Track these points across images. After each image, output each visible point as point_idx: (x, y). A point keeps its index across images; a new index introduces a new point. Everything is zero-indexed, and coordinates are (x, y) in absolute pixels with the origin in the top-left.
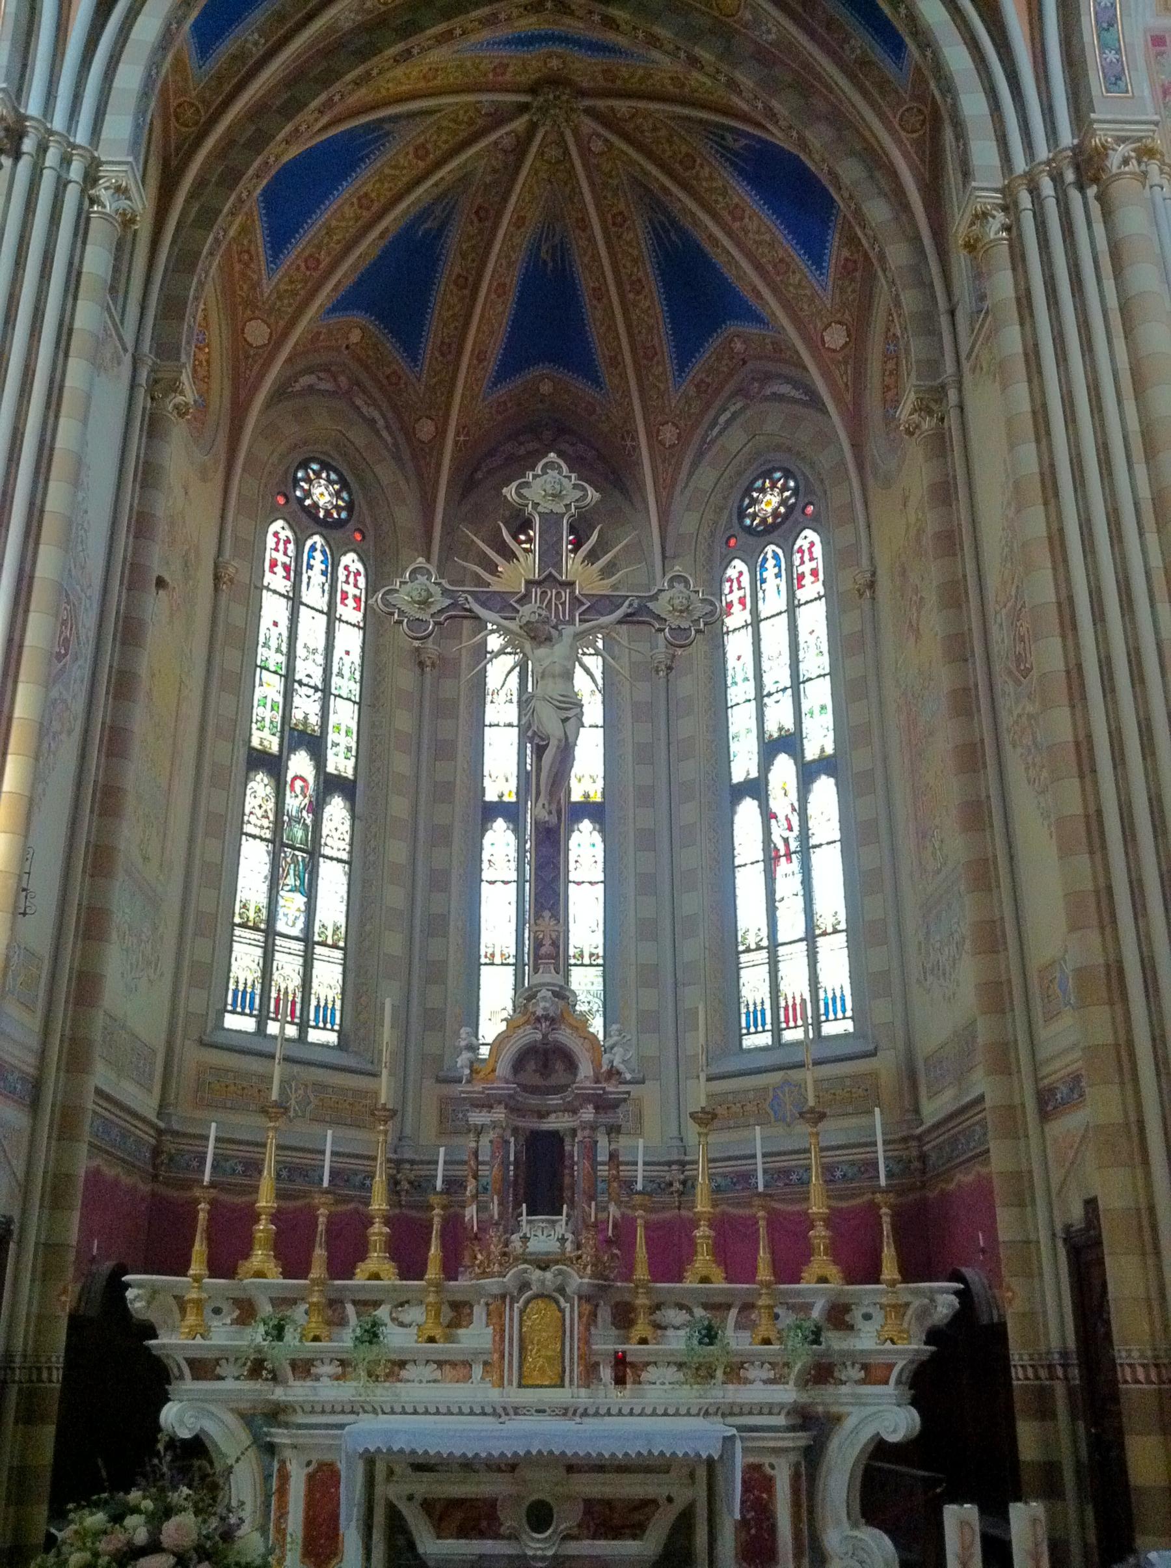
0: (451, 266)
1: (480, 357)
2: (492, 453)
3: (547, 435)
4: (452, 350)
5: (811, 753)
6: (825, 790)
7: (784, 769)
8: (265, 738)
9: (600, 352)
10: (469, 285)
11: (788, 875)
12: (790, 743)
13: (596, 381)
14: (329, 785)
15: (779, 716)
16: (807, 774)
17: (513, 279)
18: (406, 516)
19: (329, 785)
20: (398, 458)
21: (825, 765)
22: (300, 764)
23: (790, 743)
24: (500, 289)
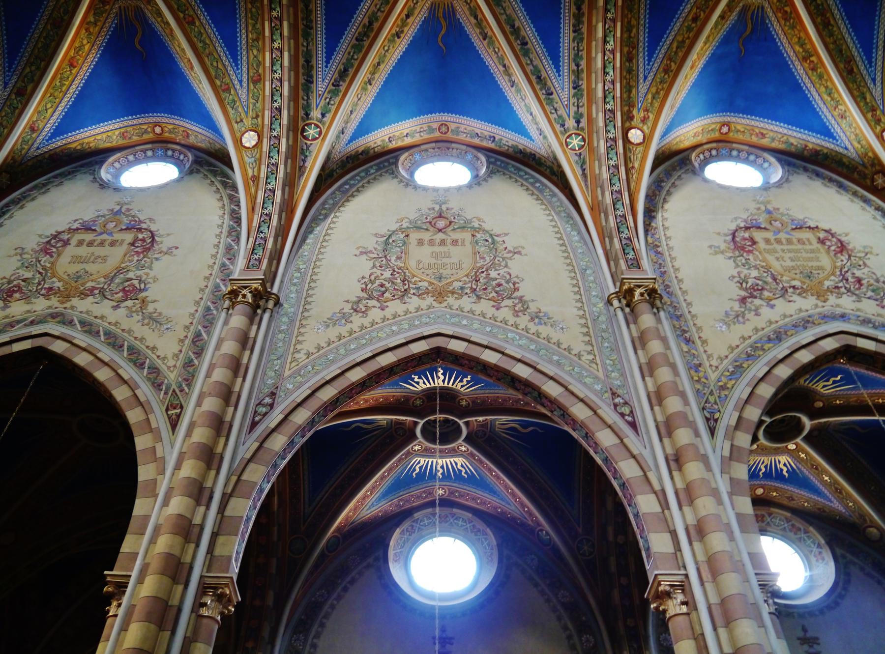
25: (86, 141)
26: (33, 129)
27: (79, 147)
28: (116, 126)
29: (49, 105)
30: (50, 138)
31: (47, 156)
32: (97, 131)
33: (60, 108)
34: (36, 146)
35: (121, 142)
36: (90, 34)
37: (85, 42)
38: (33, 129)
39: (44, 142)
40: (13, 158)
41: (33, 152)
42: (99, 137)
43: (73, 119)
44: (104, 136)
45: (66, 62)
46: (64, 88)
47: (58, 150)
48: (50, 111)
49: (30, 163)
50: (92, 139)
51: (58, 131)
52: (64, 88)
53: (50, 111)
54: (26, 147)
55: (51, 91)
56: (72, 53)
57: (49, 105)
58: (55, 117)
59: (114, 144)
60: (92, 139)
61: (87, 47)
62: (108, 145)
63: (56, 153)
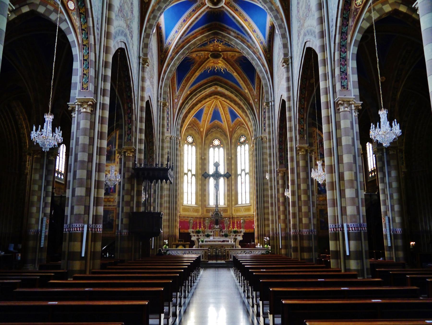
0: (205, 112)
1: (208, 121)
2: (209, 131)
4: (205, 121)
5: (246, 172)
6: (247, 176)
7: (243, 173)
8: (186, 171)
9: (223, 120)
10: (207, 114)
11: (243, 185)
12: (244, 170)
13: (222, 122)
14: (192, 175)
15: (243, 168)
16: (246, 174)
17: (212, 113)
18: (200, 141)
19: (192, 175)
21: (248, 173)
22: (189, 174)
23: (244, 170)
24: (210, 114)
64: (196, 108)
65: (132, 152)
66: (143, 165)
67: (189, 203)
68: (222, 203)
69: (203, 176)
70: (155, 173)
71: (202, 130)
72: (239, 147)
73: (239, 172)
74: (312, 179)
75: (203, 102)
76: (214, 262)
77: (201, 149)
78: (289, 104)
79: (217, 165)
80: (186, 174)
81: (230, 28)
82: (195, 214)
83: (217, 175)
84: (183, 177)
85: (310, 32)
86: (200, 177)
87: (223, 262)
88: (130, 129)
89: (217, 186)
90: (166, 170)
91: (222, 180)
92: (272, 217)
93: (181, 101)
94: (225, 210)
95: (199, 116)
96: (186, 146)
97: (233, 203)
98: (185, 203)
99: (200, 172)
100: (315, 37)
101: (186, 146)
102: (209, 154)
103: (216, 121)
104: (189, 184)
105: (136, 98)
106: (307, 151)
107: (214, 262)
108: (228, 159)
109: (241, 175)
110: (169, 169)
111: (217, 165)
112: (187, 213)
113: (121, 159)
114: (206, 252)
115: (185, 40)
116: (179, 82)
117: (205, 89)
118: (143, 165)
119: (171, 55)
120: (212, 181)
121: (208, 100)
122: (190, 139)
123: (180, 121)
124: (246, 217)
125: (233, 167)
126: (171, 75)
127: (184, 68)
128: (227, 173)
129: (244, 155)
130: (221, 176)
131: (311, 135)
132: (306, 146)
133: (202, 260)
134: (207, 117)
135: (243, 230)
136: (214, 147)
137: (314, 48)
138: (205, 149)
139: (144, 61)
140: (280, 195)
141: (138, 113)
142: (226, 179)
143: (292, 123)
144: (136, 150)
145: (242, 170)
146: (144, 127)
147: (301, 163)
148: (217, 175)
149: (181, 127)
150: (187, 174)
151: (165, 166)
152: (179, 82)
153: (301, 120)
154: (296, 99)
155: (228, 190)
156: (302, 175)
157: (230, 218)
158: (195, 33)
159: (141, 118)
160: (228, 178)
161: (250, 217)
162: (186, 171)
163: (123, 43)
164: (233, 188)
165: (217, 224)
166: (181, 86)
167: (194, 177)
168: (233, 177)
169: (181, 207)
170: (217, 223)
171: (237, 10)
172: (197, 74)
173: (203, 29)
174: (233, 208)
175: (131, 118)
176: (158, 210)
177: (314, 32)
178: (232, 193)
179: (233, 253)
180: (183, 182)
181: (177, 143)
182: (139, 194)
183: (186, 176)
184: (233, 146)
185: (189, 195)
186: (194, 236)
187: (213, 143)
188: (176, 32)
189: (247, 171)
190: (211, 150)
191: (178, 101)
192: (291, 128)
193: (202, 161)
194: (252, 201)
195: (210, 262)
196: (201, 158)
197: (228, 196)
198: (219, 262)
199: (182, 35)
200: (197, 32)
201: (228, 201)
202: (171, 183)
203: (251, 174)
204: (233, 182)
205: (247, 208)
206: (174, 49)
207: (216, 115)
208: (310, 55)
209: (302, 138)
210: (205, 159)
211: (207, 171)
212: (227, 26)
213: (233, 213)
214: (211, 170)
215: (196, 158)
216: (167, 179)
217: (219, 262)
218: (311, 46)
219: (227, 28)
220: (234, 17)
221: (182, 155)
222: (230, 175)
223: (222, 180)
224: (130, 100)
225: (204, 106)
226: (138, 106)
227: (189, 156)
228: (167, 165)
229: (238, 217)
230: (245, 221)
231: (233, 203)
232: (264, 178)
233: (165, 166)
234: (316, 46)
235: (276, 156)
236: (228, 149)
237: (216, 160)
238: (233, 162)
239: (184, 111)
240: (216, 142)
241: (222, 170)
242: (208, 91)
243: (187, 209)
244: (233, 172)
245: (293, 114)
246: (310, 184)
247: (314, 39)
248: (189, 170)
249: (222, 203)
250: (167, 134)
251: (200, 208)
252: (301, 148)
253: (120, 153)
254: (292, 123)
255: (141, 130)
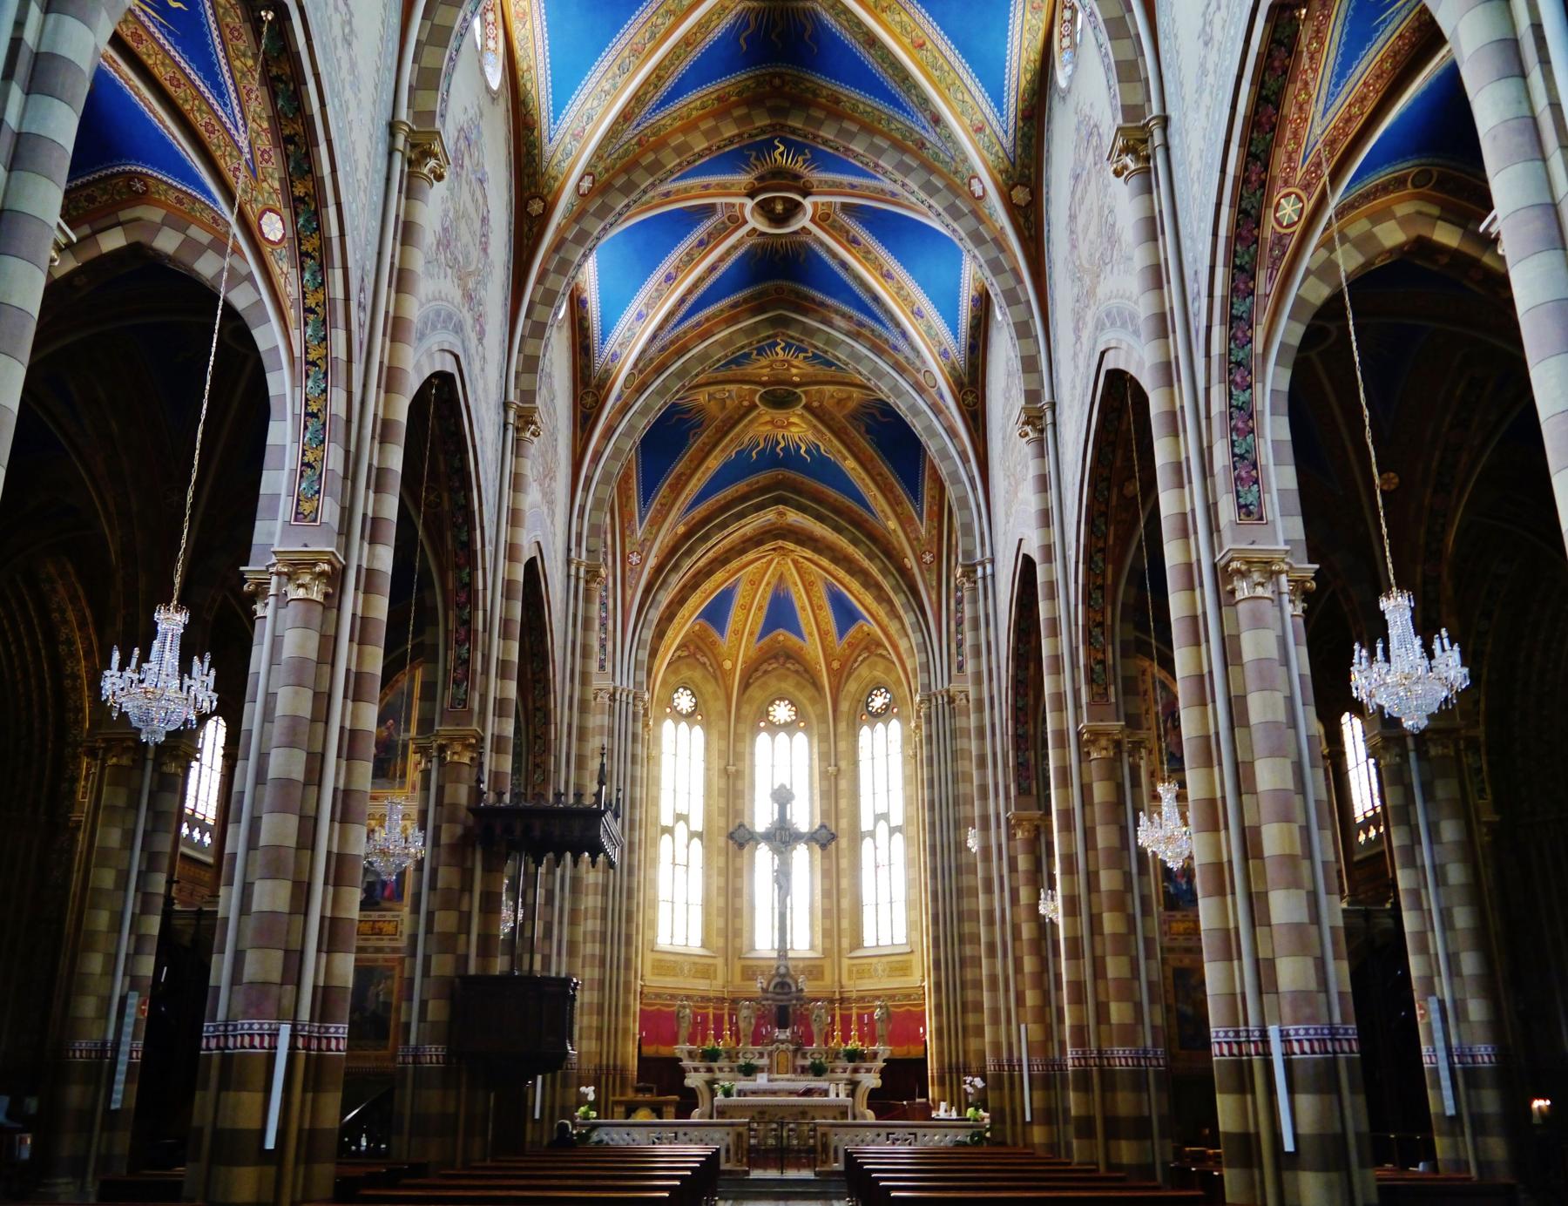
0: (738, 600)
1: (751, 634)
2: (756, 670)
3: (781, 660)
4: (738, 633)
6: (898, 837)
7: (882, 828)
9: (805, 632)
11: (883, 872)
12: (885, 817)
13: (802, 637)
14: (692, 835)
15: (881, 809)
16: (892, 831)
18: (720, 705)
19: (692, 835)
20: (716, 679)
21: (898, 829)
22: (681, 829)
23: (885, 817)
24: (760, 608)
25: (1023, 63)
26: (980, 130)
27: (1029, 76)
28: (1019, 14)
29: (959, 96)
30: (1000, 110)
31: (1021, 124)
32: (1016, 43)
33: (969, 82)
34: (1001, 134)
35: (1044, 15)
36: (889, 7)
37: (897, 18)
38: (980, 130)
39: (1003, 125)
40: (1001, 172)
41: (1008, 142)
42: (1026, 44)
43: (990, 75)
44: (1027, 35)
45: (915, 52)
46: (946, 68)
47: (1020, 106)
48: (967, 97)
49: (1019, 151)
50: (1024, 55)
51: (997, 98)
52: (946, 68)
53: (967, 97)
54: (998, 147)
55: (942, 86)
56: (907, 41)
57: (959, 96)
58: (977, 94)
59: (1043, 26)
60: (1024, 55)
61: (905, 18)
62: (1041, 36)
63: (1023, 111)
64: (707, 585)
65: (468, 746)
66: (507, 798)
67: (679, 940)
68: (802, 942)
69: (732, 839)
70: (547, 827)
71: (728, 665)
72: (865, 731)
73: (866, 824)
74: (1142, 853)
75: (735, 564)
76: (772, 1174)
77: (725, 735)
78: (1049, 572)
79: (782, 797)
80: (669, 831)
81: (830, 301)
82: (701, 986)
83: (783, 837)
84: (655, 844)
85: (1115, 318)
86: (721, 841)
87: (807, 1174)
88: (465, 663)
89: (783, 878)
90: (595, 816)
91: (801, 855)
92: (994, 999)
93: (652, 562)
94: (814, 970)
95: (716, 614)
96: (668, 725)
97: (845, 943)
98: (663, 941)
99: (722, 822)
100: (1136, 333)
101: (668, 725)
102: (752, 754)
103: (782, 635)
104: (680, 870)
105: (489, 549)
106: (1118, 744)
107: (772, 1174)
108: (824, 775)
109: (872, 834)
110: (604, 812)
111: (782, 797)
112: (669, 982)
113: (426, 774)
114: (739, 1135)
115: (672, 343)
116: (647, 493)
117: (742, 515)
118: (507, 798)
119: (619, 398)
120: (764, 857)
121: (751, 555)
122: (684, 701)
123: (648, 634)
124: (892, 997)
125: (843, 803)
126: (617, 468)
127: (667, 441)
128: (823, 826)
129: (885, 757)
130: (797, 837)
131: (1131, 687)
132: (1116, 726)
133: (724, 1166)
134: (746, 618)
135: (883, 1050)
136: (774, 728)
137: (1132, 371)
138: (738, 738)
139: (521, 420)
140: (1023, 914)
141: (497, 604)
142: (817, 848)
143: (1063, 640)
144: (482, 739)
145: (878, 817)
146: (515, 657)
147: (1100, 792)
148: (783, 837)
149: (653, 654)
150: (669, 831)
151: (589, 800)
152: (647, 493)
153: (1094, 630)
154: (1072, 553)
155: (826, 894)
156: (1103, 837)
157: (832, 1001)
158: (707, 319)
159: (506, 623)
160: (823, 847)
161: (908, 996)
162: (666, 819)
163: (449, 357)
164: (845, 883)
165: (783, 1025)
166: (655, 505)
167: (696, 842)
168: (844, 842)
169: (649, 956)
170: (782, 1020)
171: (855, 241)
172: (714, 463)
173: (733, 306)
174: (846, 962)
175: (467, 623)
176: (559, 968)
177: (1133, 317)
178: (840, 910)
179: (843, 1141)
180: (654, 862)
181: (635, 714)
182: (490, 905)
183: (666, 838)
184: (842, 727)
185: (676, 916)
186: (696, 1070)
187: (768, 714)
188: (640, 316)
189: (897, 819)
190: (763, 739)
191: (643, 561)
192: (1056, 659)
193: (730, 780)
194: (916, 936)
195: (756, 1174)
196: (725, 772)
197: (826, 913)
198: (791, 1174)
199: (661, 327)
200: (714, 316)
201: (827, 934)
202: (611, 865)
203: (912, 830)
204: (844, 863)
205: (899, 963)
206: (631, 374)
207: (780, 613)
208: (1120, 399)
209: (1098, 697)
210: (738, 775)
211: (746, 822)
212: (819, 296)
213: (845, 981)
214: (763, 817)
215: (707, 769)
216: (596, 849)
217: (791, 1174)
218: (1122, 367)
219: (822, 304)
220: (844, 264)
221: (653, 760)
222: (834, 837)
223: (801, 855)
224: (467, 555)
225: (738, 580)
226: (495, 578)
227: (680, 761)
228: (598, 795)
229: (862, 999)
230: (889, 1016)
231: (845, 943)
232: (961, 846)
233: (589, 800)
234: (1140, 364)
235: (1006, 765)
236: (823, 738)
237: (782, 779)
238: (843, 784)
239: (665, 598)
240: (782, 712)
241: (803, 817)
242: (753, 524)
243: (669, 963)
244: (844, 823)
245: (1064, 607)
246: (1134, 870)
247: (1132, 340)
248: (679, 817)
249: (802, 942)
250: (599, 682)
251: (720, 962)
252: (1096, 735)
253: (423, 750)
254: (1063, 640)
255: (504, 665)
